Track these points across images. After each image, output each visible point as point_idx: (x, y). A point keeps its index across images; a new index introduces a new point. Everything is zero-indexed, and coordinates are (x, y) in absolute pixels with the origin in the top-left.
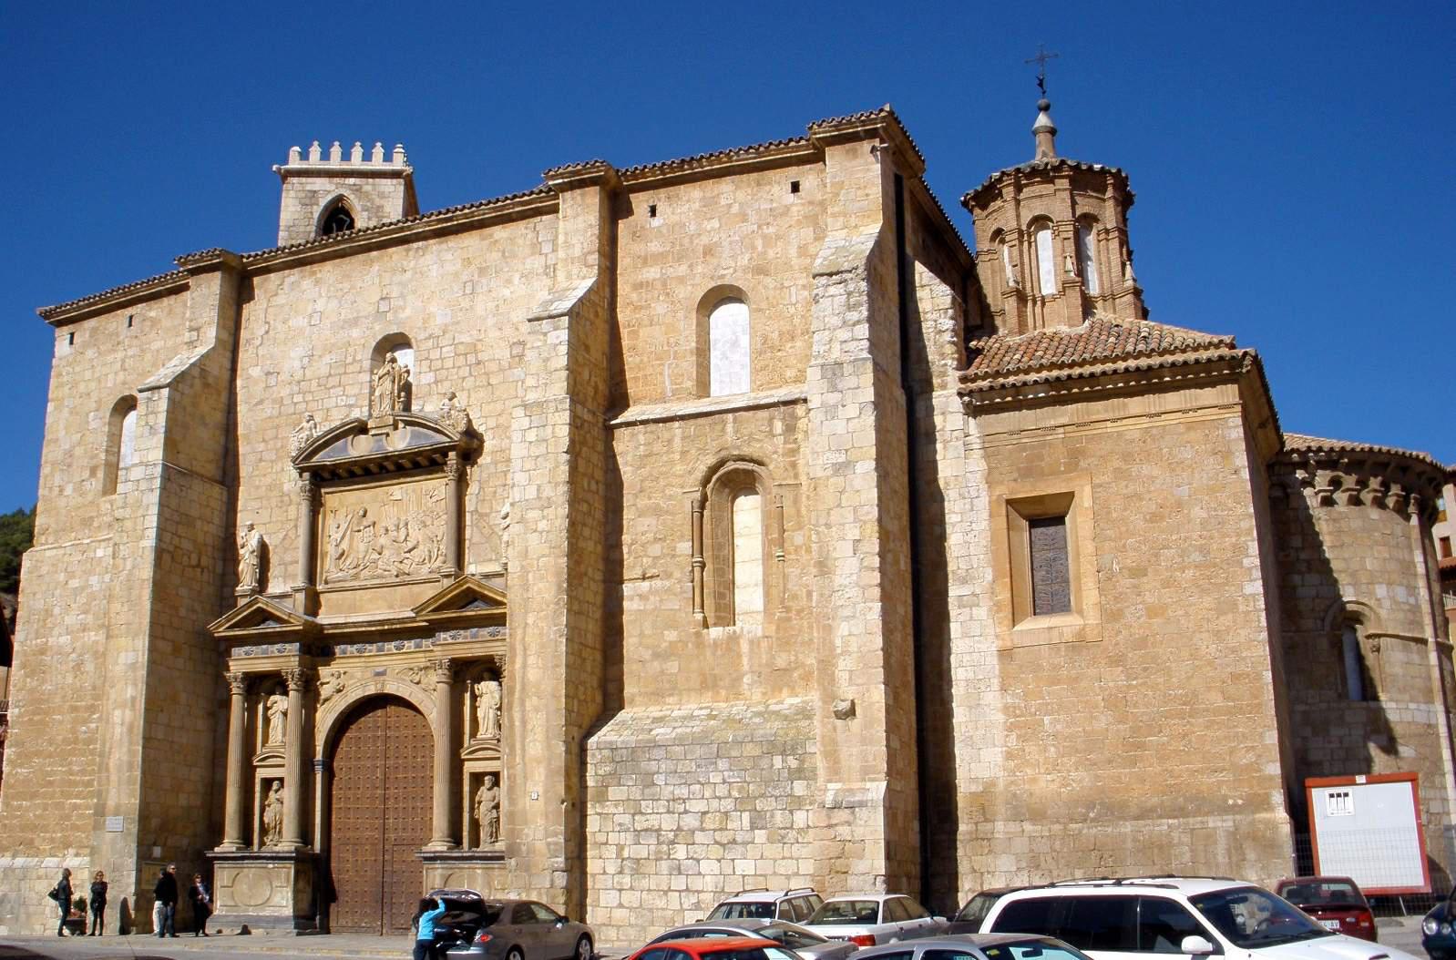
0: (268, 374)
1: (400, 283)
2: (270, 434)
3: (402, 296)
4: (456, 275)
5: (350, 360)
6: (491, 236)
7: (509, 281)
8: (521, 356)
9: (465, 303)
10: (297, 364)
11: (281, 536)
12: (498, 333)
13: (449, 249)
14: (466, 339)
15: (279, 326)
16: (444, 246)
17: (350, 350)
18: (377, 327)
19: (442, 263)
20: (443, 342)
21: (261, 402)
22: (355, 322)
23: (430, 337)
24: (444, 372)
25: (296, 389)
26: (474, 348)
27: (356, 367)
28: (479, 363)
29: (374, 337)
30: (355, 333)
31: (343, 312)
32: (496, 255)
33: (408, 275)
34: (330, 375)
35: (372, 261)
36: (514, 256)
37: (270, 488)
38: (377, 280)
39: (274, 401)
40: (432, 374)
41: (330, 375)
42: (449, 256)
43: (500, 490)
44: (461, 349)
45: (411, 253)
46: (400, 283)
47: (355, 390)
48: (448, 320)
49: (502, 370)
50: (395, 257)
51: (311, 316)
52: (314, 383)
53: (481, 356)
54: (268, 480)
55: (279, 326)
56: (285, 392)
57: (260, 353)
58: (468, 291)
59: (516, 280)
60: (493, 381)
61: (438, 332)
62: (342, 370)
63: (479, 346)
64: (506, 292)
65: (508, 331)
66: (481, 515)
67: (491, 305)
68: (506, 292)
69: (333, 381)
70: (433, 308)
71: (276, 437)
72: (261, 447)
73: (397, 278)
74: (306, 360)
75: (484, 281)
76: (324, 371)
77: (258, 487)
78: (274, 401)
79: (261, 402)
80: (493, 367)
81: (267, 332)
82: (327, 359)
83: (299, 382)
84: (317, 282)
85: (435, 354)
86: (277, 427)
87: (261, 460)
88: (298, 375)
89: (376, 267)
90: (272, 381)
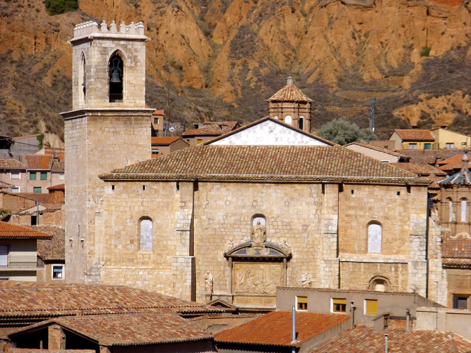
0: (209, 219)
1: (261, 197)
2: (212, 240)
3: (262, 201)
4: (282, 198)
5: (242, 220)
6: (295, 187)
7: (301, 204)
8: (306, 230)
9: (286, 208)
10: (221, 218)
11: (218, 275)
12: (298, 221)
13: (279, 189)
14: (286, 220)
15: (213, 203)
16: (277, 187)
17: (242, 216)
18: (253, 210)
19: (276, 193)
20: (278, 220)
21: (207, 229)
22: (244, 207)
23: (273, 218)
24: (278, 231)
25: (221, 226)
26: (289, 224)
27: (245, 223)
28: (291, 229)
29: (251, 213)
30: (244, 211)
31: (239, 203)
32: (296, 194)
33: (264, 194)
34: (235, 224)
35: (249, 187)
36: (303, 196)
37: (213, 259)
38: (252, 194)
39: (213, 229)
40: (274, 230)
41: (235, 224)
42: (279, 191)
43: (299, 271)
44: (285, 224)
45: (265, 187)
46: (261, 197)
47: (245, 231)
48: (279, 213)
49: (299, 233)
50: (258, 187)
51: (226, 201)
52: (229, 225)
53: (292, 227)
54: (212, 256)
55: (213, 203)
56: (217, 227)
57: (205, 210)
58: (287, 204)
59: (304, 204)
60: (296, 236)
61: (275, 216)
62: (239, 223)
63: (291, 224)
64: (301, 208)
65: (302, 221)
66: (293, 278)
67: (295, 211)
68: (301, 208)
69: (235, 226)
70: (274, 208)
71: (214, 242)
72: (208, 244)
73: (260, 195)
74: (225, 217)
75: (292, 202)
76: (233, 222)
77: (207, 258)
78: (213, 229)
79: (207, 229)
80: (296, 231)
81: (208, 204)
82: (233, 218)
83: (222, 224)
84: (227, 190)
85: (275, 224)
86: (214, 238)
87: (208, 249)
88: (222, 221)
89: (251, 189)
90: (211, 222)
